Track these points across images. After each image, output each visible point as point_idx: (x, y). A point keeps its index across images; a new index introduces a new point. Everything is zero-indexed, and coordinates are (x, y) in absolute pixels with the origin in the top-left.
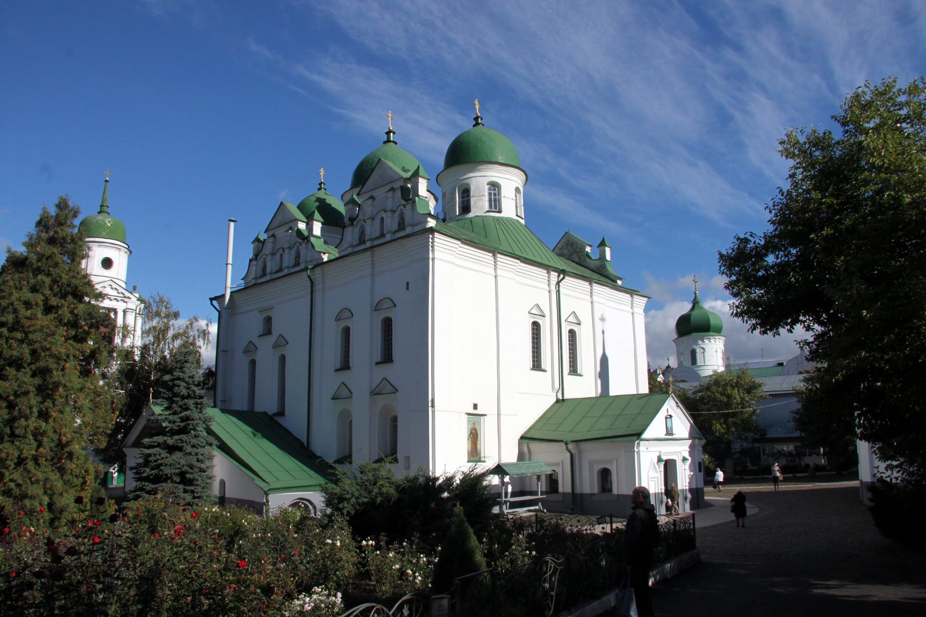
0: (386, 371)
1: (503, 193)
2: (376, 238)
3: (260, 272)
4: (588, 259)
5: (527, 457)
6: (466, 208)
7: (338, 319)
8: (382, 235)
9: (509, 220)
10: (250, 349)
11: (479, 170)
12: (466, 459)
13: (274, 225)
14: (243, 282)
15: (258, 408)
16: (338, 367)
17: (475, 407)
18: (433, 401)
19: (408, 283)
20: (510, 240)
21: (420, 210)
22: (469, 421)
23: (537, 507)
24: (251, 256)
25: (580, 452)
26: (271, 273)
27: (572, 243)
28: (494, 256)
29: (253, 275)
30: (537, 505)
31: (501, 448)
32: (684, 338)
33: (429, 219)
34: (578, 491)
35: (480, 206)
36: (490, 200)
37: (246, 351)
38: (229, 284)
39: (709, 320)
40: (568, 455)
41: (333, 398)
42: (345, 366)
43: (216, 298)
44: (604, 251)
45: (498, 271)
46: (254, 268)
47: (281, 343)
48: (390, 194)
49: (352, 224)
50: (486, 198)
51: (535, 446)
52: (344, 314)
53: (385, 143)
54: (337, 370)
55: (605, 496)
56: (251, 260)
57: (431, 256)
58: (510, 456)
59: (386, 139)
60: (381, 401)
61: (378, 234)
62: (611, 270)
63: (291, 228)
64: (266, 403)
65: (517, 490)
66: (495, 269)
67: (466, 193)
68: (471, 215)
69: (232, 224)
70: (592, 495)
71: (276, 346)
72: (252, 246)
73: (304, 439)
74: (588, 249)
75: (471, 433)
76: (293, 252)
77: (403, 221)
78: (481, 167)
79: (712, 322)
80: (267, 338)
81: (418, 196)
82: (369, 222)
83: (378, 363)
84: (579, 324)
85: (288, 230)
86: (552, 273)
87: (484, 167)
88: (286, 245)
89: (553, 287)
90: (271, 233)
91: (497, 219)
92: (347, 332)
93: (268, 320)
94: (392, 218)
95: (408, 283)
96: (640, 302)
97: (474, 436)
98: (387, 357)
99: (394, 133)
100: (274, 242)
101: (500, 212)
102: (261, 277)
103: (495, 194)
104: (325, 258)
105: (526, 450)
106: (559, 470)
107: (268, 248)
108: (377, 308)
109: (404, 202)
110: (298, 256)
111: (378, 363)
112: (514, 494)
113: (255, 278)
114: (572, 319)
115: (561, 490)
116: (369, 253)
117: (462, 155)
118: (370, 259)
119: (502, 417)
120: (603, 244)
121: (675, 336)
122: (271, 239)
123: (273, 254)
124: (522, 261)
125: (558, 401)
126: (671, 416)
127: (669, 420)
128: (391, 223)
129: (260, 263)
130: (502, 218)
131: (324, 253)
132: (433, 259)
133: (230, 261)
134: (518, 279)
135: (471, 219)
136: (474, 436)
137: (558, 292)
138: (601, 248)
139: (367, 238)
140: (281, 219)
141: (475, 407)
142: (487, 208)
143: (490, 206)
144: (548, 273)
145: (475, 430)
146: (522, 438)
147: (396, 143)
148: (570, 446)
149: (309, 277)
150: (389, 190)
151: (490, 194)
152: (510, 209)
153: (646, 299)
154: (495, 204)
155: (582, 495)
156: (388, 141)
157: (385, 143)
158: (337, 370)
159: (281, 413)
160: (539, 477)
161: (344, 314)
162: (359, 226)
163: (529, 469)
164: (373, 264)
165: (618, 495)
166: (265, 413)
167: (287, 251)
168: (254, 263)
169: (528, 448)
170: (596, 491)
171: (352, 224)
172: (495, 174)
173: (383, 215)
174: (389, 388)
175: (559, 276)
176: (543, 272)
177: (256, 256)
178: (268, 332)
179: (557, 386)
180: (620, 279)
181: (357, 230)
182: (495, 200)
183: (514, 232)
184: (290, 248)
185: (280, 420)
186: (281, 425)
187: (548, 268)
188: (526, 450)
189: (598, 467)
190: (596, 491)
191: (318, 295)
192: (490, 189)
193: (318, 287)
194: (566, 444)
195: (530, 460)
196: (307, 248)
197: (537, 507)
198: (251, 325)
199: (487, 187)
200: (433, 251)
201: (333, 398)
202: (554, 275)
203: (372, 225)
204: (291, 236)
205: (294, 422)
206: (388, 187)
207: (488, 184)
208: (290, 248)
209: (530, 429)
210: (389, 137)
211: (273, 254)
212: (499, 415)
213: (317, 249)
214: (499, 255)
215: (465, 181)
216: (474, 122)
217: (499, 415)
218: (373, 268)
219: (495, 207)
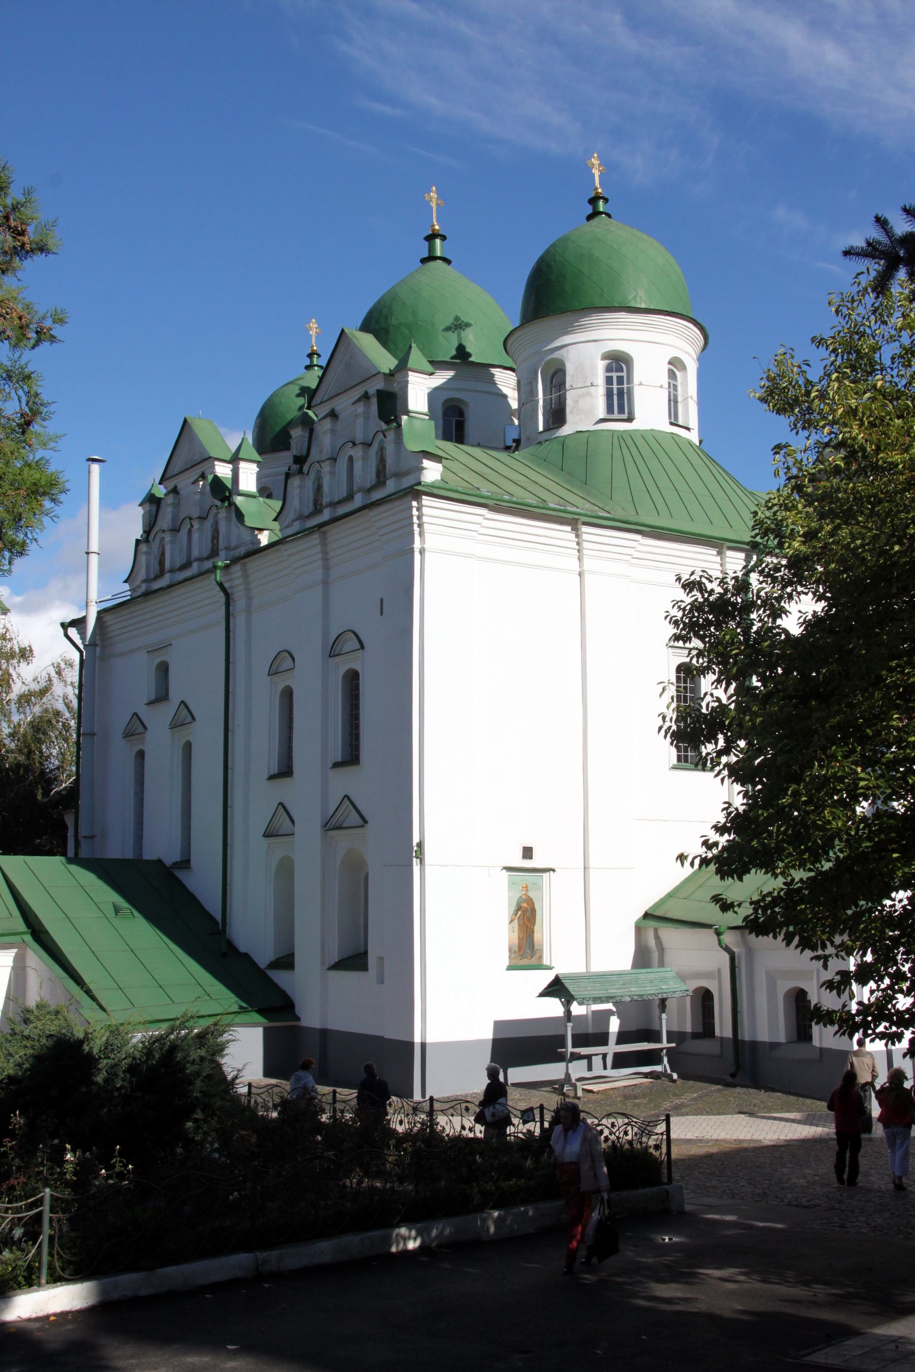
0: (348, 782)
1: (637, 377)
2: (340, 502)
3: (155, 568)
5: (655, 956)
6: (557, 416)
7: (273, 672)
8: (350, 497)
10: (136, 728)
11: (584, 328)
12: (506, 963)
13: (176, 467)
14: (127, 587)
15: (149, 854)
16: (275, 770)
17: (528, 853)
18: (420, 845)
19: (382, 600)
20: (636, 483)
21: (412, 445)
22: (512, 884)
23: (658, 1068)
24: (138, 533)
25: (750, 951)
26: (172, 571)
28: (575, 529)
29: (142, 574)
30: (659, 1062)
31: (596, 941)
33: (426, 463)
34: (746, 1035)
35: (587, 409)
36: (609, 394)
37: (129, 734)
38: (94, 595)
40: (727, 956)
41: (266, 835)
42: (285, 771)
43: (75, 623)
45: (586, 560)
46: (143, 559)
47: (185, 717)
48: (360, 408)
49: (300, 472)
50: (600, 391)
51: (671, 936)
52: (281, 662)
53: (424, 261)
54: (271, 778)
55: (799, 1051)
56: (138, 541)
57: (417, 545)
58: (615, 954)
59: (426, 255)
60: (344, 841)
61: (344, 493)
63: (203, 476)
64: (161, 845)
65: (633, 1028)
67: (557, 378)
68: (566, 430)
69: (95, 467)
70: (774, 1046)
71: (175, 725)
72: (140, 511)
73: (219, 918)
75: (519, 908)
76: (208, 525)
77: (384, 467)
78: (585, 321)
80: (162, 706)
81: (407, 412)
82: (326, 467)
83: (336, 765)
85: (196, 482)
86: (729, 553)
87: (594, 319)
88: (195, 513)
90: (171, 484)
91: (621, 435)
92: (288, 695)
93: (163, 669)
94: (365, 459)
95: (382, 600)
97: (526, 915)
98: (351, 756)
100: (177, 505)
101: (630, 419)
102: (157, 578)
103: (620, 380)
104: (264, 539)
105: (652, 942)
106: (713, 987)
107: (165, 520)
108: (333, 651)
109: (384, 426)
110: (215, 537)
111: (336, 765)
112: (623, 1038)
113: (147, 581)
115: (717, 1033)
116: (315, 539)
117: (554, 294)
118: (318, 549)
119: (592, 873)
122: (171, 499)
123: (175, 530)
128: (364, 472)
129: (155, 546)
130: (630, 434)
131: (261, 530)
132: (422, 551)
133: (94, 547)
135: (564, 440)
136: (526, 915)
139: (355, 488)
140: (187, 456)
141: (528, 853)
142: (601, 412)
143: (610, 409)
144: (720, 553)
145: (530, 901)
146: (647, 916)
147: (448, 261)
148: (729, 938)
149: (221, 585)
150: (358, 400)
151: (609, 380)
152: (650, 413)
154: (620, 400)
155: (754, 1044)
156: (431, 258)
157: (424, 261)
158: (271, 778)
159: (185, 863)
160: (663, 1002)
161: (281, 662)
162: (312, 475)
163: (653, 983)
164: (326, 560)
165: (821, 1050)
166: (159, 862)
167: (196, 525)
168: (143, 548)
169: (657, 937)
170: (781, 1037)
171: (300, 472)
173: (350, 451)
174: (354, 819)
177: (147, 532)
178: (162, 696)
181: (309, 483)
182: (621, 393)
183: (653, 463)
184: (202, 518)
185: (181, 875)
186: (184, 888)
188: (652, 942)
189: (785, 986)
190: (781, 1037)
191: (239, 622)
192: (609, 369)
193: (239, 604)
194: (718, 933)
195: (662, 964)
196: (228, 519)
197: (658, 1068)
198: (133, 680)
199: (601, 365)
200: (421, 534)
201: (266, 835)
203: (332, 474)
204: (202, 493)
205: (203, 882)
206: (358, 393)
207: (606, 356)
208: (202, 518)
209: (670, 896)
210: (431, 248)
211: (175, 530)
212: (586, 868)
213: (249, 522)
214: (585, 529)
215: (555, 355)
216: (589, 210)
217: (586, 868)
218: (326, 568)
219: (621, 411)
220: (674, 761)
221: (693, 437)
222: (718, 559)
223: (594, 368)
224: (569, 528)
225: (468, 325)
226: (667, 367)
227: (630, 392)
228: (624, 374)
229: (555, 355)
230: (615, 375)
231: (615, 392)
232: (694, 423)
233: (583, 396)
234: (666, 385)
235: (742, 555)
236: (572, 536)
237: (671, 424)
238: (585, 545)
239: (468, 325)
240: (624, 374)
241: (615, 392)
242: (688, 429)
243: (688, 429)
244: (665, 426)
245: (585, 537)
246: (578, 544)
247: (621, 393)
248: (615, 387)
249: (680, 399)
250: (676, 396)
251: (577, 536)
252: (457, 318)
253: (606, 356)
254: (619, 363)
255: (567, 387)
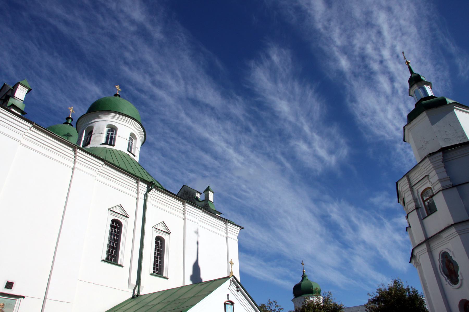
1: (118, 134)
4: (197, 202)
9: (120, 153)
11: (102, 117)
27: (187, 193)
28: (74, 150)
32: (298, 298)
39: (312, 287)
44: (208, 194)
45: (77, 164)
50: (104, 136)
62: (212, 207)
66: (74, 163)
67: (90, 133)
68: (89, 146)
74: (198, 195)
78: (103, 115)
79: (314, 287)
84: (169, 234)
87: (106, 114)
89: (142, 196)
96: (234, 232)
99: (72, 120)
101: (113, 145)
103: (112, 134)
114: (161, 227)
119: (47, 300)
120: (208, 190)
121: (292, 297)
124: (105, 164)
125: (133, 297)
126: (232, 303)
127: (229, 307)
130: (112, 150)
134: (99, 178)
137: (145, 201)
138: (206, 193)
142: (104, 141)
144: (137, 182)
152: (121, 145)
153: (239, 228)
154: (110, 140)
156: (67, 123)
172: (113, 119)
175: (148, 187)
176: (132, 182)
179: (134, 281)
180: (220, 213)
182: (112, 137)
187: (138, 179)
192: (109, 131)
199: (106, 130)
202: (143, 187)
207: (109, 126)
212: (45, 299)
215: (91, 125)
220: (104, 258)
221: (137, 159)
222: (136, 185)
223: (103, 129)
224: (72, 149)
225: (71, 136)
226: (129, 136)
227: (115, 137)
228: (114, 133)
229: (91, 125)
230: (110, 133)
231: (110, 137)
232: (137, 153)
233: (97, 136)
234: (128, 139)
235: (146, 186)
236: (73, 153)
237: (128, 151)
238: (77, 157)
239: (71, 136)
240: (114, 133)
241: (110, 137)
242: (135, 156)
243: (135, 156)
244: (125, 150)
245: (78, 154)
246: (75, 157)
247: (112, 137)
248: (110, 135)
249: (133, 147)
250: (132, 145)
251: (75, 154)
252: (68, 133)
253: (109, 126)
254: (112, 129)
255: (93, 133)
